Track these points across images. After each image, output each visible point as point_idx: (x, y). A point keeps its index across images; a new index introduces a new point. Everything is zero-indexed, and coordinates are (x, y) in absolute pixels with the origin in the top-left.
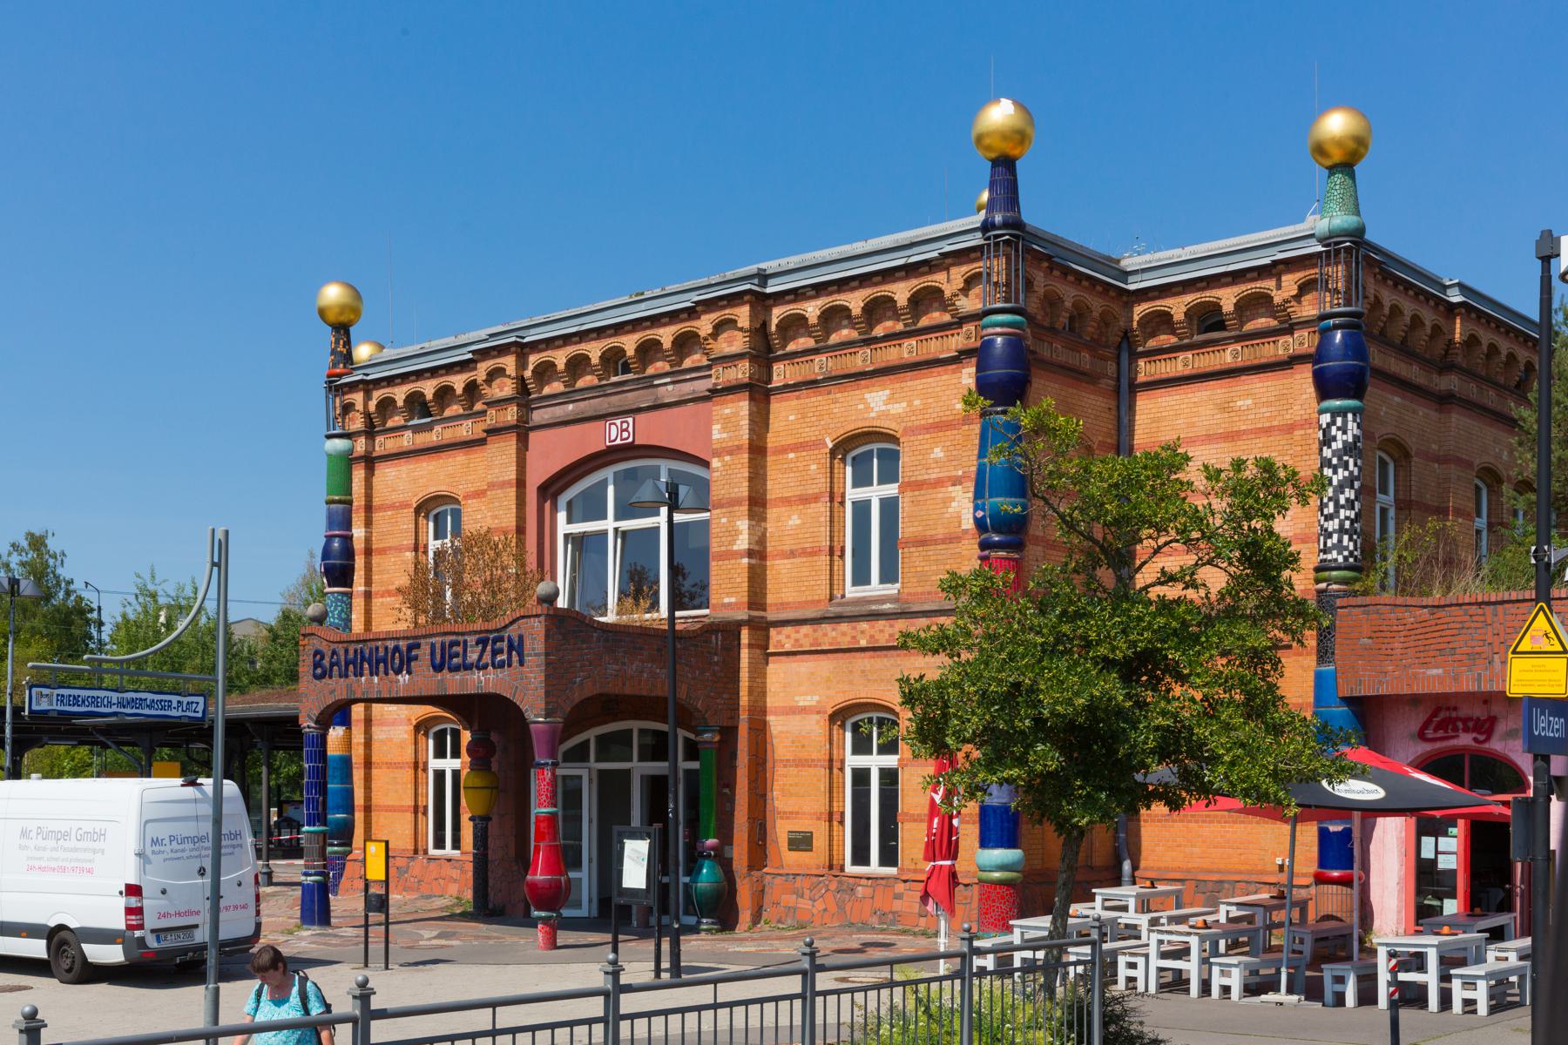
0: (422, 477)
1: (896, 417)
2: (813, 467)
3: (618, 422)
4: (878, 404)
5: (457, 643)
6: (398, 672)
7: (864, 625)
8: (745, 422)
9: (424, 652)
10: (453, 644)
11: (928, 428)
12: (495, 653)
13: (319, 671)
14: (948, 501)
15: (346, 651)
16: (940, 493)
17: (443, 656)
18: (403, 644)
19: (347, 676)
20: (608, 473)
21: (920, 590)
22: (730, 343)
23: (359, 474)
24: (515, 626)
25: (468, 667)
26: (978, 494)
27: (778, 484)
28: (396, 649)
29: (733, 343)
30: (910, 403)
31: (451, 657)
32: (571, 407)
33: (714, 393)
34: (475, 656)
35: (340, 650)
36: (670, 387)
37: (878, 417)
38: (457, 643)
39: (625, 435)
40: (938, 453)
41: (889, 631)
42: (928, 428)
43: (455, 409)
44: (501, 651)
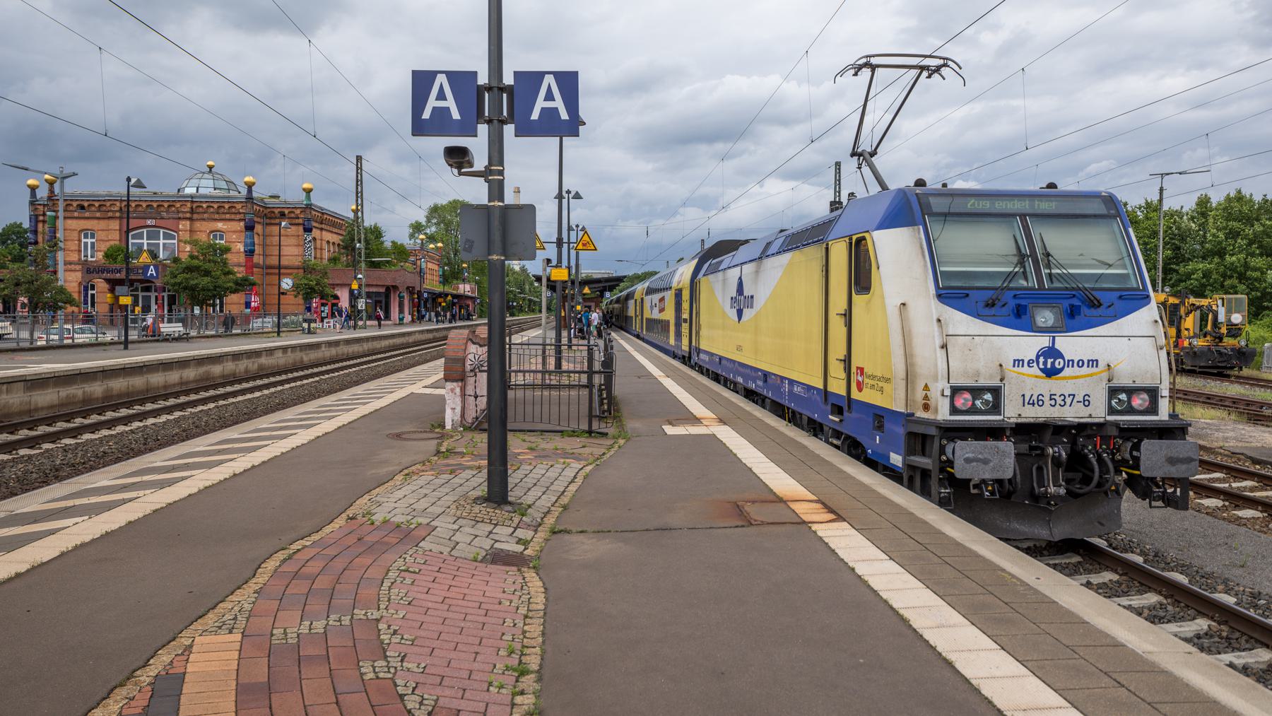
4: (220, 225)
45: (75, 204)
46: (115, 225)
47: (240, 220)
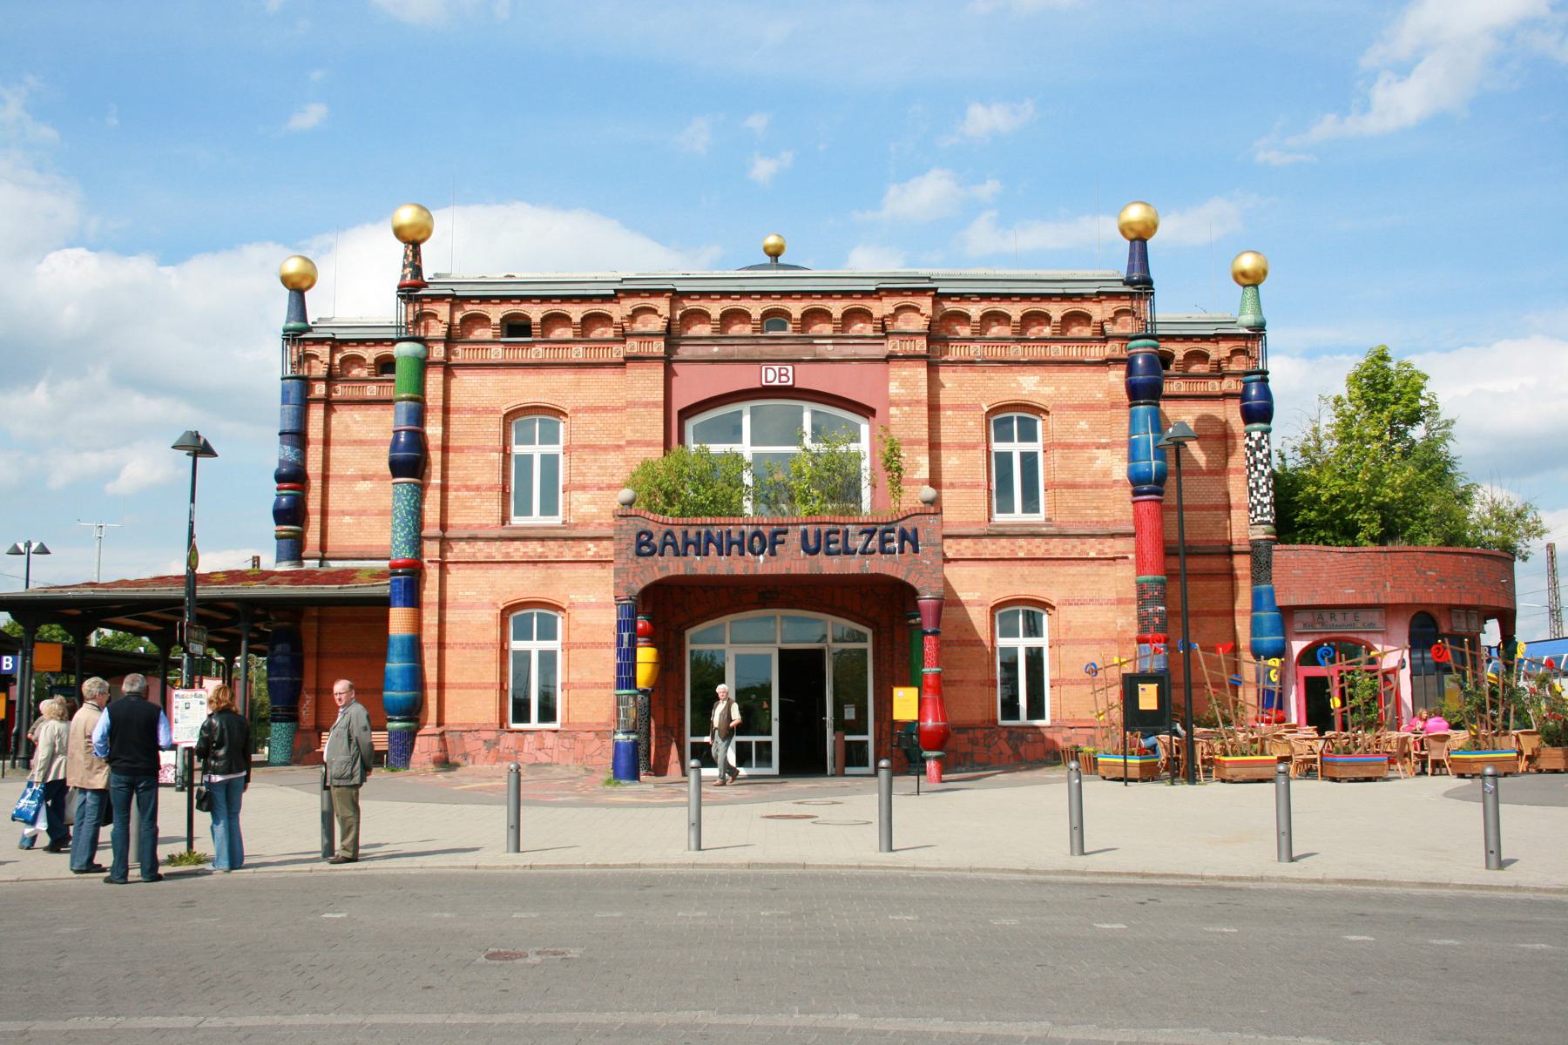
1: (1043, 396)
3: (776, 368)
4: (1028, 386)
7: (1022, 542)
9: (794, 537)
10: (829, 533)
11: (1075, 407)
12: (883, 541)
13: (645, 549)
14: (1092, 460)
15: (686, 533)
16: (1087, 454)
18: (766, 531)
19: (685, 554)
20: (746, 408)
22: (907, 322)
23: (434, 379)
25: (848, 551)
26: (1132, 458)
27: (947, 434)
28: (757, 534)
29: (917, 323)
30: (1058, 388)
31: (829, 543)
32: (716, 349)
33: (890, 358)
36: (830, 348)
38: (837, 532)
42: (1075, 407)
44: (891, 540)
45: (496, 313)
46: (648, 382)
47: (1106, 363)
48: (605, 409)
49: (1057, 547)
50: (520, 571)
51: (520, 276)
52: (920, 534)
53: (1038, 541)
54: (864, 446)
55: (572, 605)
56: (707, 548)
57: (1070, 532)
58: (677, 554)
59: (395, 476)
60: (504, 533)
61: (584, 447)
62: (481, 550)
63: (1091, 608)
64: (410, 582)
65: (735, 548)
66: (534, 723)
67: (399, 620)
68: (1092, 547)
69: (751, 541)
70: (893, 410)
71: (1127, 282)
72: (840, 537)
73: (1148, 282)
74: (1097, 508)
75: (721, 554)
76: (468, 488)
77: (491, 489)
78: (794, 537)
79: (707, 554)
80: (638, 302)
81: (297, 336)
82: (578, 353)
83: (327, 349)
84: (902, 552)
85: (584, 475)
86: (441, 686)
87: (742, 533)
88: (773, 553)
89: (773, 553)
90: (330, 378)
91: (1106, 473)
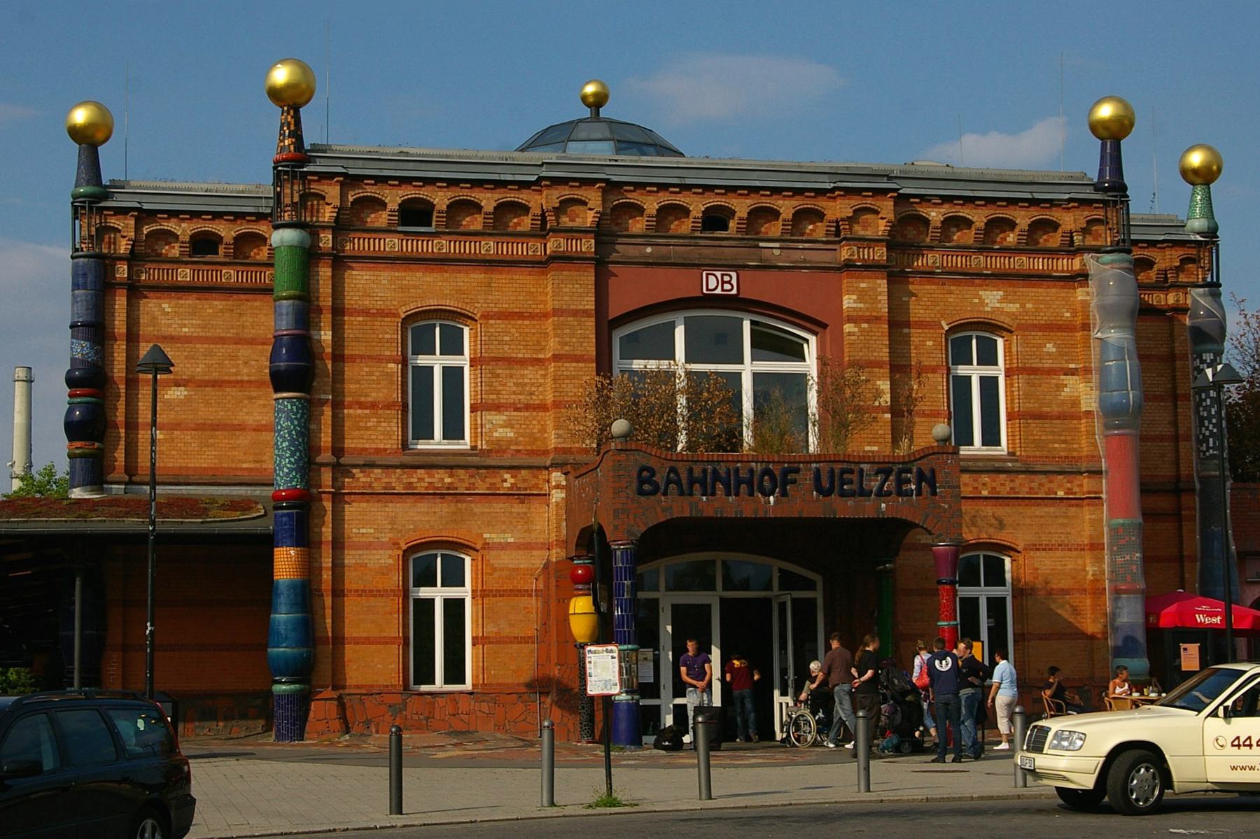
0: (415, 287)
2: (930, 343)
3: (718, 274)
4: (992, 300)
5: (852, 472)
6: (766, 494)
7: (985, 478)
8: (884, 298)
9: (806, 477)
10: (843, 472)
12: (900, 482)
13: (646, 487)
15: (691, 470)
17: (832, 482)
19: (691, 494)
21: (1038, 454)
24: (925, 461)
25: (865, 493)
26: (1103, 386)
28: (766, 472)
32: (649, 250)
34: (875, 485)
35: (683, 470)
36: (777, 252)
37: (993, 312)
38: (852, 472)
39: (727, 287)
40: (1050, 347)
41: (1009, 485)
43: (475, 223)
44: (909, 481)
45: (393, 198)
46: (577, 289)
48: (520, 316)
49: (1022, 485)
50: (423, 506)
51: (415, 151)
52: (939, 477)
53: (1003, 476)
54: (810, 365)
55: (487, 546)
56: (714, 487)
57: (1039, 468)
58: (682, 494)
59: (276, 391)
60: (407, 459)
61: (497, 359)
62: (378, 479)
63: (1059, 553)
64: (301, 515)
65: (743, 488)
66: (439, 684)
67: (286, 562)
68: (1060, 486)
69: (761, 481)
70: (848, 328)
71: (1097, 187)
72: (855, 477)
73: (1123, 188)
74: (1064, 442)
75: (729, 494)
76: (361, 405)
77: (389, 406)
78: (806, 477)
79: (713, 494)
80: (566, 192)
81: (94, 202)
82: (488, 247)
83: (132, 222)
84: (919, 493)
85: (498, 393)
86: (406, 644)
87: (751, 471)
88: (784, 493)
89: (784, 493)
90: (133, 258)
91: (1075, 402)
